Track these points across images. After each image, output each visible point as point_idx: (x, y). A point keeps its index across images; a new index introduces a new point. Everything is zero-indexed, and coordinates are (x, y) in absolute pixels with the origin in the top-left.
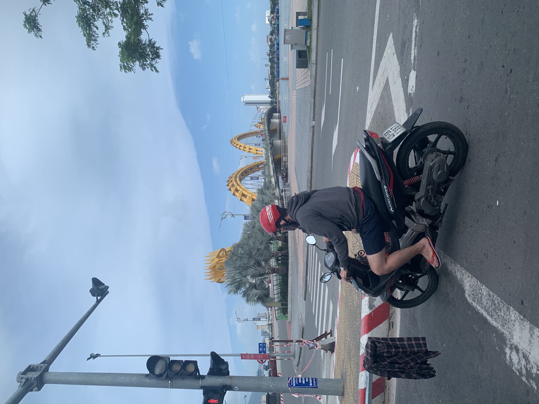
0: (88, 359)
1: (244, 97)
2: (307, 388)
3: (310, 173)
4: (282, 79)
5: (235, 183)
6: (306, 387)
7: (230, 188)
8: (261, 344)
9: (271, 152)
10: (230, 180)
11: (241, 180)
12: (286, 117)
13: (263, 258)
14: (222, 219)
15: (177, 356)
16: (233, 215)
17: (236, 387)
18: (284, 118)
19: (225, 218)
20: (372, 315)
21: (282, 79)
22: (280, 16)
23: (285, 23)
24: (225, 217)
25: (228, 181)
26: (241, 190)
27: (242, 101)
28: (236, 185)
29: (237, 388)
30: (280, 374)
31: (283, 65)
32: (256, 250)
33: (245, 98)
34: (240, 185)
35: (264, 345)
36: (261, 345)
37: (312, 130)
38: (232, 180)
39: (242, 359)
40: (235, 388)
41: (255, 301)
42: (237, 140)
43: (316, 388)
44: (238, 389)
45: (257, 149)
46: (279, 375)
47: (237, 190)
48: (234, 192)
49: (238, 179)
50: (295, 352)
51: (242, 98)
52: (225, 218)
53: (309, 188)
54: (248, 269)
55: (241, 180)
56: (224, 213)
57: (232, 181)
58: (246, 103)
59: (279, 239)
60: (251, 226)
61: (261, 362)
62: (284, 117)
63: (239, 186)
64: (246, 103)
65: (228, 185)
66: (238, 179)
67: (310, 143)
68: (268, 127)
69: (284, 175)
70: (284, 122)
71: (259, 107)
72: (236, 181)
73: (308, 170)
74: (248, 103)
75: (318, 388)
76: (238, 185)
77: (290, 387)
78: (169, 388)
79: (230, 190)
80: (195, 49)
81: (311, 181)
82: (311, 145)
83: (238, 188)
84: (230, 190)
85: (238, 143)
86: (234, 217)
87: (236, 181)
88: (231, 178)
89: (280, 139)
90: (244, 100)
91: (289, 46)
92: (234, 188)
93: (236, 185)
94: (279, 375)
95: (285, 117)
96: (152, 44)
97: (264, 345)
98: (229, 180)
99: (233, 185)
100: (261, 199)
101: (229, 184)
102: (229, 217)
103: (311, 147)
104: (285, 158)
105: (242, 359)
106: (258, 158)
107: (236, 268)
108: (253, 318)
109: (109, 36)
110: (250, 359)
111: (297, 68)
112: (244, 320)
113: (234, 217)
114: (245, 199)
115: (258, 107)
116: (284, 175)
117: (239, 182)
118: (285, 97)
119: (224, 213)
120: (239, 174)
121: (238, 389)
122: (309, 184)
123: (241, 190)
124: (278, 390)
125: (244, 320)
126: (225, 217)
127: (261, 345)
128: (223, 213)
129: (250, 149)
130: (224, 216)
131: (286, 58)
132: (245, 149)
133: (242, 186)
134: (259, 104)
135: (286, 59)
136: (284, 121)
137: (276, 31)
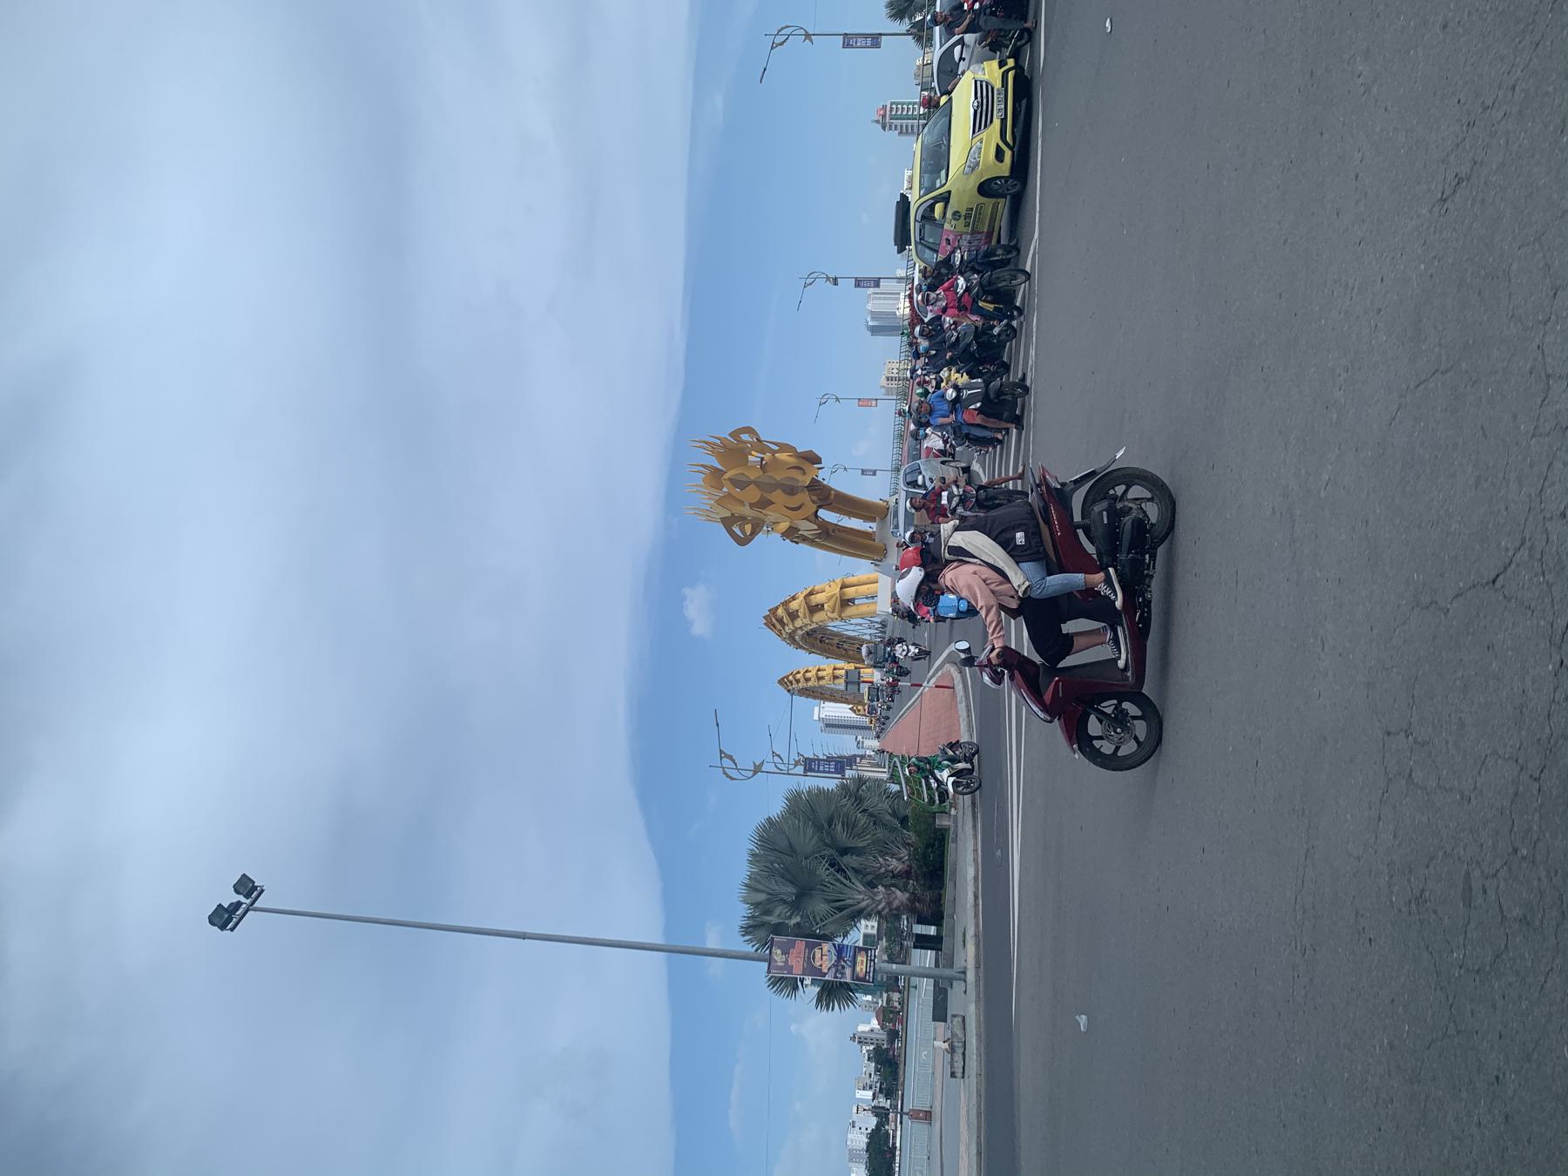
16: (808, 36)
19: (782, 44)
24: (785, 41)
27: (816, 718)
33: (825, 709)
51: (816, 709)
52: (782, 44)
58: (827, 725)
64: (827, 725)
71: (863, 742)
90: (822, 716)
106: (874, 402)
115: (859, 743)
126: (785, 41)
128: (779, 31)
130: (779, 39)
132: (820, 673)
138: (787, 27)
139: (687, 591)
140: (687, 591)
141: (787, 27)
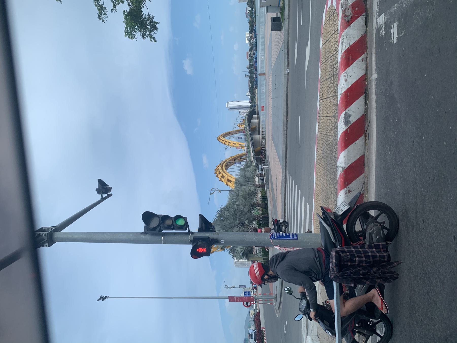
0: (98, 300)
1: (228, 103)
2: (288, 240)
3: (285, 117)
4: (260, 75)
5: (221, 171)
6: (287, 239)
7: (217, 175)
8: (246, 293)
9: (252, 144)
10: (217, 169)
11: (226, 169)
12: (264, 106)
13: (246, 218)
14: (210, 195)
15: (173, 298)
16: (220, 191)
17: (222, 240)
18: (262, 107)
19: (213, 193)
20: (348, 131)
21: (260, 75)
22: (257, 34)
23: (261, 28)
24: (214, 192)
25: (215, 170)
26: (226, 176)
27: (227, 107)
28: (222, 172)
29: (223, 241)
30: (264, 328)
31: (260, 63)
32: (240, 212)
33: (229, 104)
34: (226, 172)
35: (249, 293)
36: (246, 293)
37: (286, 78)
38: (219, 168)
39: (229, 301)
40: (221, 241)
41: (240, 256)
42: (222, 137)
43: (297, 240)
44: (224, 242)
45: (240, 143)
46: (263, 329)
47: (223, 177)
48: (221, 178)
49: (223, 167)
50: (276, 295)
51: (227, 104)
52: (213, 193)
53: (285, 132)
54: (233, 228)
55: (226, 169)
56: (213, 189)
57: (218, 170)
58: (230, 108)
59: (260, 206)
60: (235, 195)
61: (247, 306)
62: (262, 106)
63: (225, 173)
64: (230, 108)
65: (216, 173)
66: (223, 167)
67: (285, 89)
68: (248, 124)
69: (263, 155)
70: (262, 111)
72: (222, 169)
73: (284, 115)
74: (232, 108)
75: (298, 240)
76: (224, 172)
77: (272, 239)
78: (162, 244)
79: (217, 176)
80: (187, 66)
81: (287, 125)
82: (286, 91)
83: (224, 175)
84: (217, 176)
85: (223, 140)
86: (221, 192)
87: (222, 169)
88: (218, 167)
89: (259, 134)
90: (228, 106)
91: (264, 9)
92: (220, 174)
93: (222, 172)
94: (263, 329)
95: (263, 107)
96: (150, 18)
97: (249, 293)
98: (216, 169)
99: (220, 173)
100: (244, 174)
101: (216, 172)
102: (216, 193)
103: (286, 93)
104: (264, 141)
105: (229, 301)
107: (223, 228)
108: (239, 286)
109: (116, 11)
110: (237, 301)
111: (272, 30)
112: (232, 287)
113: (221, 192)
114: (230, 183)
116: (263, 155)
117: (225, 170)
118: (262, 89)
119: (213, 189)
120: (224, 164)
121: (224, 242)
122: (285, 128)
123: (226, 176)
124: (261, 242)
125: (232, 287)
126: (214, 192)
127: (246, 293)
128: (212, 189)
129: (234, 144)
130: (212, 192)
131: (262, 57)
132: (229, 144)
133: (227, 173)
134: (240, 109)
135: (263, 58)
136: (262, 110)
137: (254, 48)
138: (214, 188)
139: (184, 61)
140: (184, 61)
141: (214, 188)
